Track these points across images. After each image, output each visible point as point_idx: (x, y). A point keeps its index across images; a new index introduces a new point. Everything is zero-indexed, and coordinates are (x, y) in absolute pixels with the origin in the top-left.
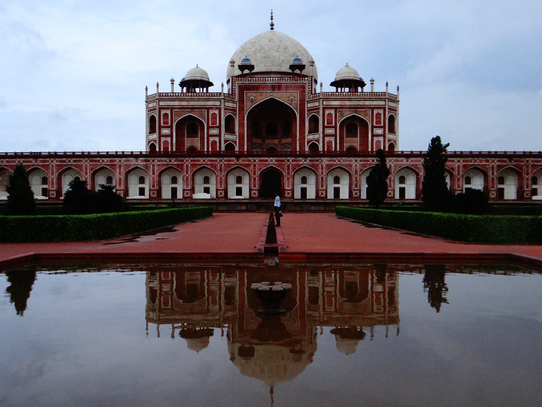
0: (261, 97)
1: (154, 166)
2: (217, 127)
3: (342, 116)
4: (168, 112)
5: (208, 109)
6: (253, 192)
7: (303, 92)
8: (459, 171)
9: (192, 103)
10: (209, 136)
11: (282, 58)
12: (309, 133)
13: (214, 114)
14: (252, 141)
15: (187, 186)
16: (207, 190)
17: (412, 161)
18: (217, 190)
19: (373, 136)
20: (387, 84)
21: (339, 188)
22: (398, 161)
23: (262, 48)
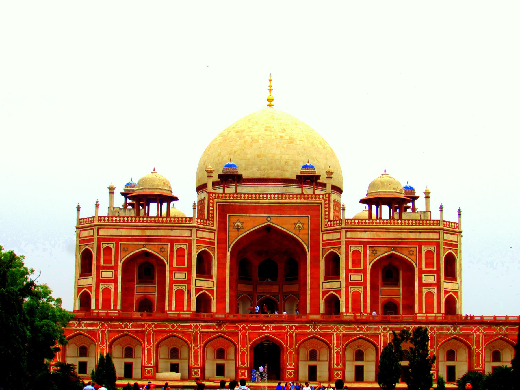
1: (103, 332)
3: (375, 254)
5: (172, 241)
6: (240, 371)
7: (319, 216)
9: (148, 233)
10: (172, 282)
11: (286, 157)
12: (325, 279)
13: (181, 250)
14: (237, 287)
15: (149, 362)
16: (175, 368)
17: (461, 330)
19: (421, 285)
22: (442, 329)
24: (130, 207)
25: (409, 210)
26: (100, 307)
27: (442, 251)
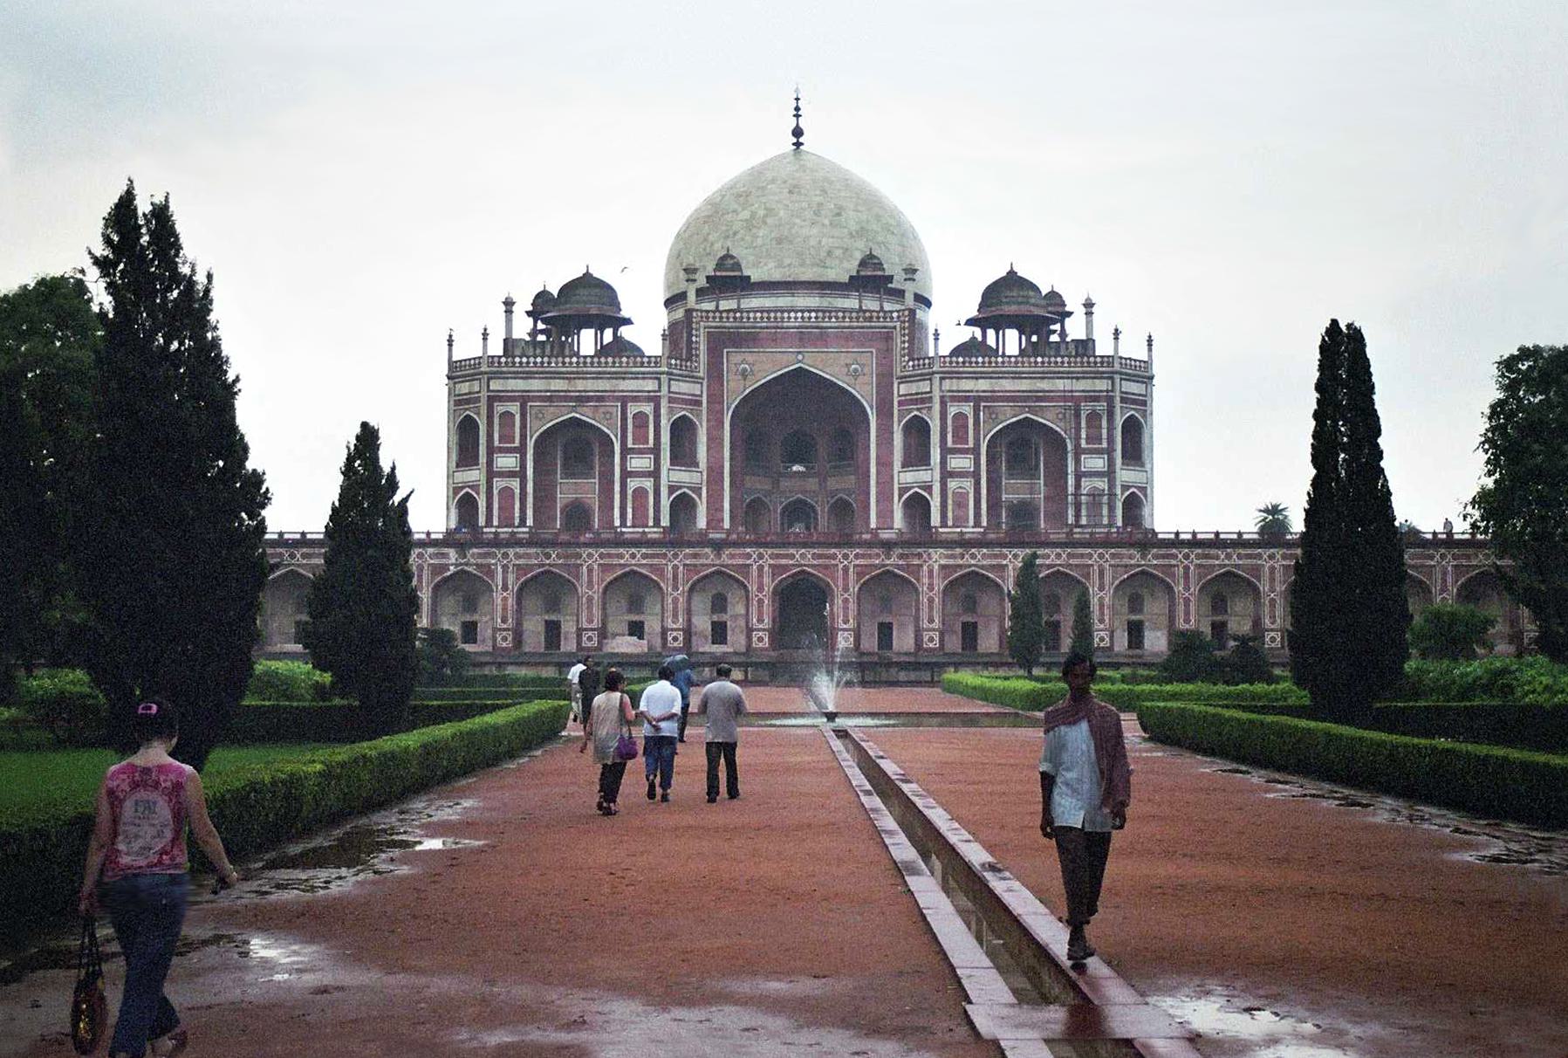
0: (767, 365)
1: (505, 567)
2: (650, 451)
4: (514, 408)
7: (889, 350)
8: (1272, 580)
9: (580, 385)
10: (626, 475)
13: (640, 418)
15: (590, 621)
16: (636, 629)
18: (664, 632)
19: (1079, 476)
20: (1117, 333)
21: (975, 625)
23: (770, 212)
24: (542, 338)
25: (1054, 338)
26: (495, 523)
27: (1118, 410)
